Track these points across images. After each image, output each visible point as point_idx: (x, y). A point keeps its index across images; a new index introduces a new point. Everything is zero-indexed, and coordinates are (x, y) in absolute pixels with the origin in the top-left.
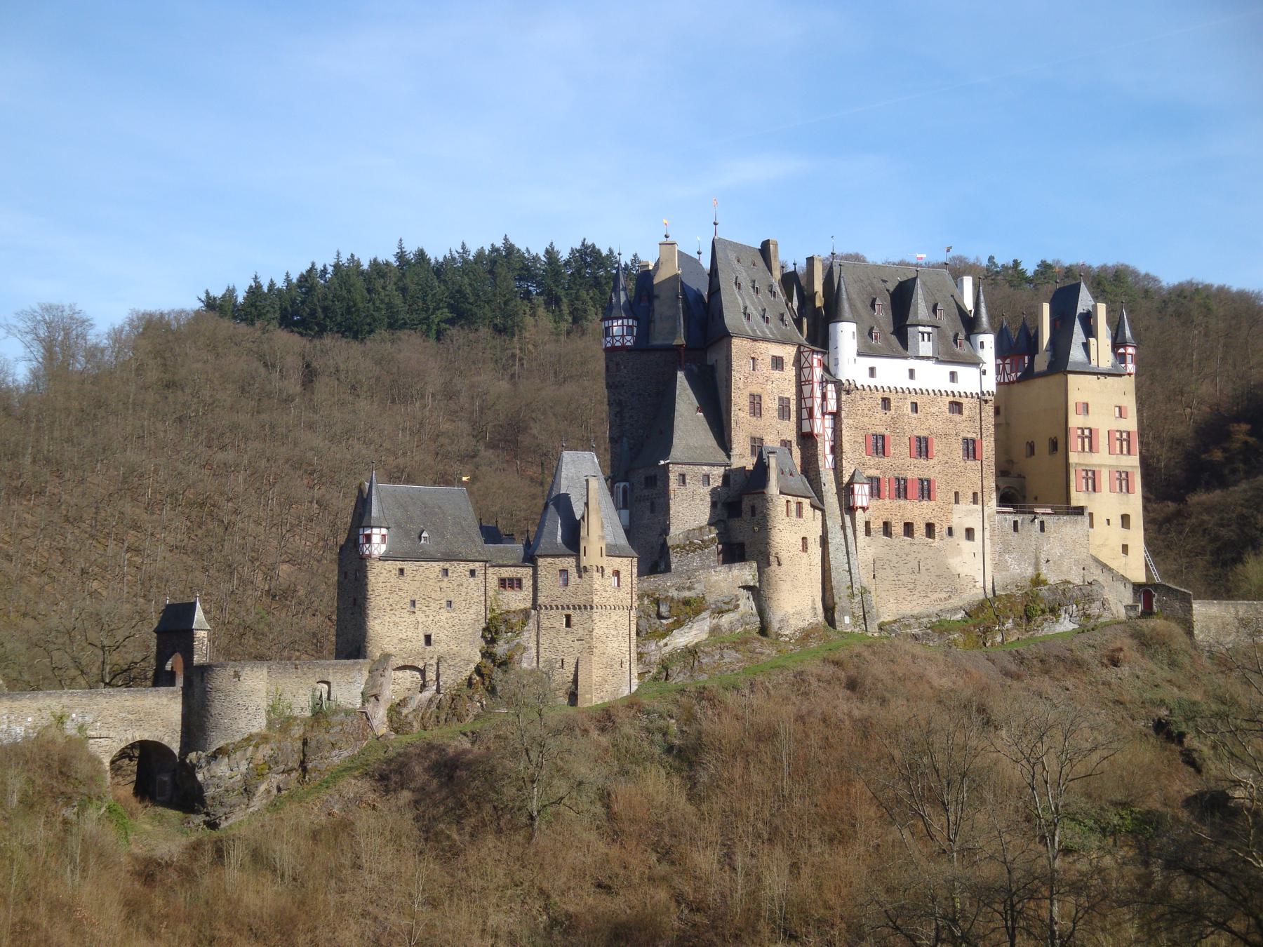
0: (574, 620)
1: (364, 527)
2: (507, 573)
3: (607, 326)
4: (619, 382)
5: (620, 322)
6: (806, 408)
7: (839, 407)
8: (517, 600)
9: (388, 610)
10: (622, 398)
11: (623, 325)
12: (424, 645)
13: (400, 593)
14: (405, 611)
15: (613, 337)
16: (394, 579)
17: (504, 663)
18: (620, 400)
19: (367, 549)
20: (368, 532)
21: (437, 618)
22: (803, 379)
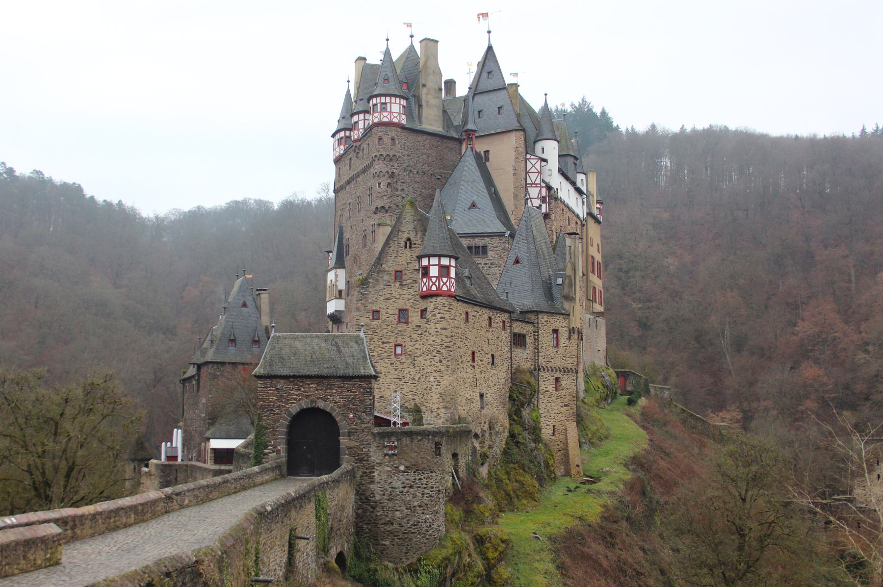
0: (563, 383)
1: (440, 256)
2: (518, 328)
4: (394, 155)
5: (398, 100)
8: (523, 357)
9: (460, 363)
10: (395, 171)
11: (400, 104)
12: (480, 407)
14: (469, 364)
15: (391, 112)
16: (463, 326)
18: (393, 173)
19: (445, 284)
20: (445, 261)
21: (487, 373)
22: (529, 181)
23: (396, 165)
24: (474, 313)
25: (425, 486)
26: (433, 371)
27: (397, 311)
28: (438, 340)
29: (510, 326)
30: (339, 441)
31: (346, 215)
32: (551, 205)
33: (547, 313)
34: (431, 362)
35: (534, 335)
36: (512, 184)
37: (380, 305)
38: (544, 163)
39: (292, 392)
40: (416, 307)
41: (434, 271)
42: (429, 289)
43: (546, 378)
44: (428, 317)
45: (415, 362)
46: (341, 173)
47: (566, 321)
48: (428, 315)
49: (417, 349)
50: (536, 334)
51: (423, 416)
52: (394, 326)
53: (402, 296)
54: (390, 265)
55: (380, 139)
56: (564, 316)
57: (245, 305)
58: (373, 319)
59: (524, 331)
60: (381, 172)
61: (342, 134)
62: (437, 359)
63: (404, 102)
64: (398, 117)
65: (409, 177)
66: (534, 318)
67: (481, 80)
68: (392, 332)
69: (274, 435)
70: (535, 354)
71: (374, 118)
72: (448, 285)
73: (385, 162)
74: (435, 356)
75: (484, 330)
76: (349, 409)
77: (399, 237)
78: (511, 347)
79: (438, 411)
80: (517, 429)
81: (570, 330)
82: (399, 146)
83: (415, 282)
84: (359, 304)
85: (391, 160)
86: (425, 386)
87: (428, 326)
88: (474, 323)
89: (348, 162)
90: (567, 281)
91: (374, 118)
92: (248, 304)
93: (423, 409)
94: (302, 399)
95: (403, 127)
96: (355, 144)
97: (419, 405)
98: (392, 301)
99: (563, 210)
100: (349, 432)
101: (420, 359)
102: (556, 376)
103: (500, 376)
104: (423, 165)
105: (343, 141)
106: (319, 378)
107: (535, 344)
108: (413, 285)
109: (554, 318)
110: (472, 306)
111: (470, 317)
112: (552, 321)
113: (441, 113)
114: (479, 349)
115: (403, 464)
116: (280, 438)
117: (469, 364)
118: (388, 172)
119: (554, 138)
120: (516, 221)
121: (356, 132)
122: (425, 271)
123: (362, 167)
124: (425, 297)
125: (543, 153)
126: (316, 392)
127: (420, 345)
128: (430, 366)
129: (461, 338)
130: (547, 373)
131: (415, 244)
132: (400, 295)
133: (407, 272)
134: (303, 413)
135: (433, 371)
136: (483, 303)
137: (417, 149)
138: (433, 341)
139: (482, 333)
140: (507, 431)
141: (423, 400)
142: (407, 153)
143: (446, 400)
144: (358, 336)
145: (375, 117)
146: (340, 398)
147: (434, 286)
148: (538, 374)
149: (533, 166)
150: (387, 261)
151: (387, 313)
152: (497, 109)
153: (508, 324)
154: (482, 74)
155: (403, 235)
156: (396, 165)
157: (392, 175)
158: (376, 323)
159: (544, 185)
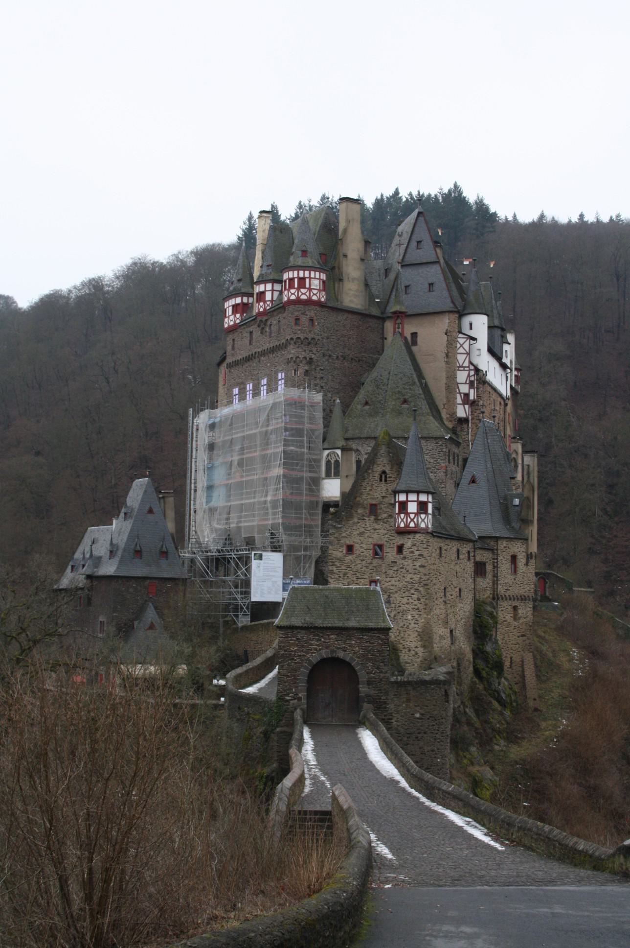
0: (520, 612)
1: (418, 492)
3: (301, 275)
4: (313, 339)
5: (317, 274)
6: (460, 393)
7: (477, 397)
10: (313, 356)
11: (320, 279)
13: (440, 577)
15: (310, 289)
16: (437, 561)
17: (498, 666)
18: (311, 359)
19: (423, 520)
20: (423, 498)
23: (314, 350)
24: (445, 548)
25: (437, 732)
26: (411, 610)
27: (371, 546)
28: (416, 578)
29: (474, 556)
30: (359, 689)
32: (480, 391)
33: (506, 538)
34: (408, 600)
35: (494, 562)
36: (444, 374)
37: (354, 540)
38: (472, 342)
39: (313, 642)
40: (392, 542)
41: (412, 508)
42: (407, 526)
43: (504, 607)
44: (404, 553)
45: (391, 599)
46: (236, 345)
47: (524, 546)
48: (406, 551)
49: (393, 585)
50: (495, 561)
51: (400, 654)
52: (369, 561)
53: (378, 531)
55: (297, 320)
56: (522, 541)
57: (150, 511)
58: (347, 554)
59: (484, 558)
60: (298, 357)
61: (238, 300)
62: (415, 597)
63: (324, 277)
64: (318, 295)
65: (328, 363)
66: (493, 544)
67: (409, 250)
68: (367, 567)
69: (295, 683)
70: (493, 582)
71: (290, 294)
72: (426, 522)
73: (302, 345)
74: (413, 594)
75: (453, 563)
76: (368, 659)
77: (375, 470)
78: (474, 578)
79: (416, 650)
80: (481, 665)
81: (528, 555)
82: (318, 327)
83: (391, 516)
84: (332, 538)
85: (309, 344)
86: (402, 624)
87: (406, 563)
88: (446, 558)
89: (248, 335)
91: (290, 294)
92: (155, 510)
93: (401, 646)
94: (323, 650)
96: (259, 319)
97: (395, 642)
98: (366, 535)
99: (489, 392)
100: (368, 681)
101: (396, 595)
102: (514, 605)
103: (465, 609)
104: (343, 348)
105: (240, 308)
106: (340, 630)
107: (494, 571)
108: (389, 520)
109: (512, 543)
110: (444, 540)
111: (443, 552)
112: (510, 546)
113: (362, 288)
114: (450, 583)
115: (419, 712)
116: (301, 686)
117: (441, 600)
118: (305, 358)
119: (484, 312)
120: (448, 416)
121: (261, 304)
123: (267, 346)
124: (402, 532)
125: (471, 328)
126: (336, 643)
127: (395, 581)
128: (408, 603)
129: (436, 574)
130: (505, 602)
131: (390, 477)
132: (375, 530)
133: (383, 506)
134: (323, 661)
135: (411, 610)
136: (453, 536)
137: (337, 331)
138: (411, 579)
139: (452, 567)
140: (471, 666)
141: (399, 638)
142: (326, 335)
143: (425, 639)
144: (375, 591)
145: (292, 294)
146: (359, 648)
147: (412, 523)
148: (497, 603)
149: (461, 346)
150: (361, 494)
151: (361, 547)
152: (428, 286)
153: (472, 554)
154: (411, 243)
155: (379, 468)
156: (314, 350)
157: (310, 362)
158: (350, 557)
159: (472, 367)
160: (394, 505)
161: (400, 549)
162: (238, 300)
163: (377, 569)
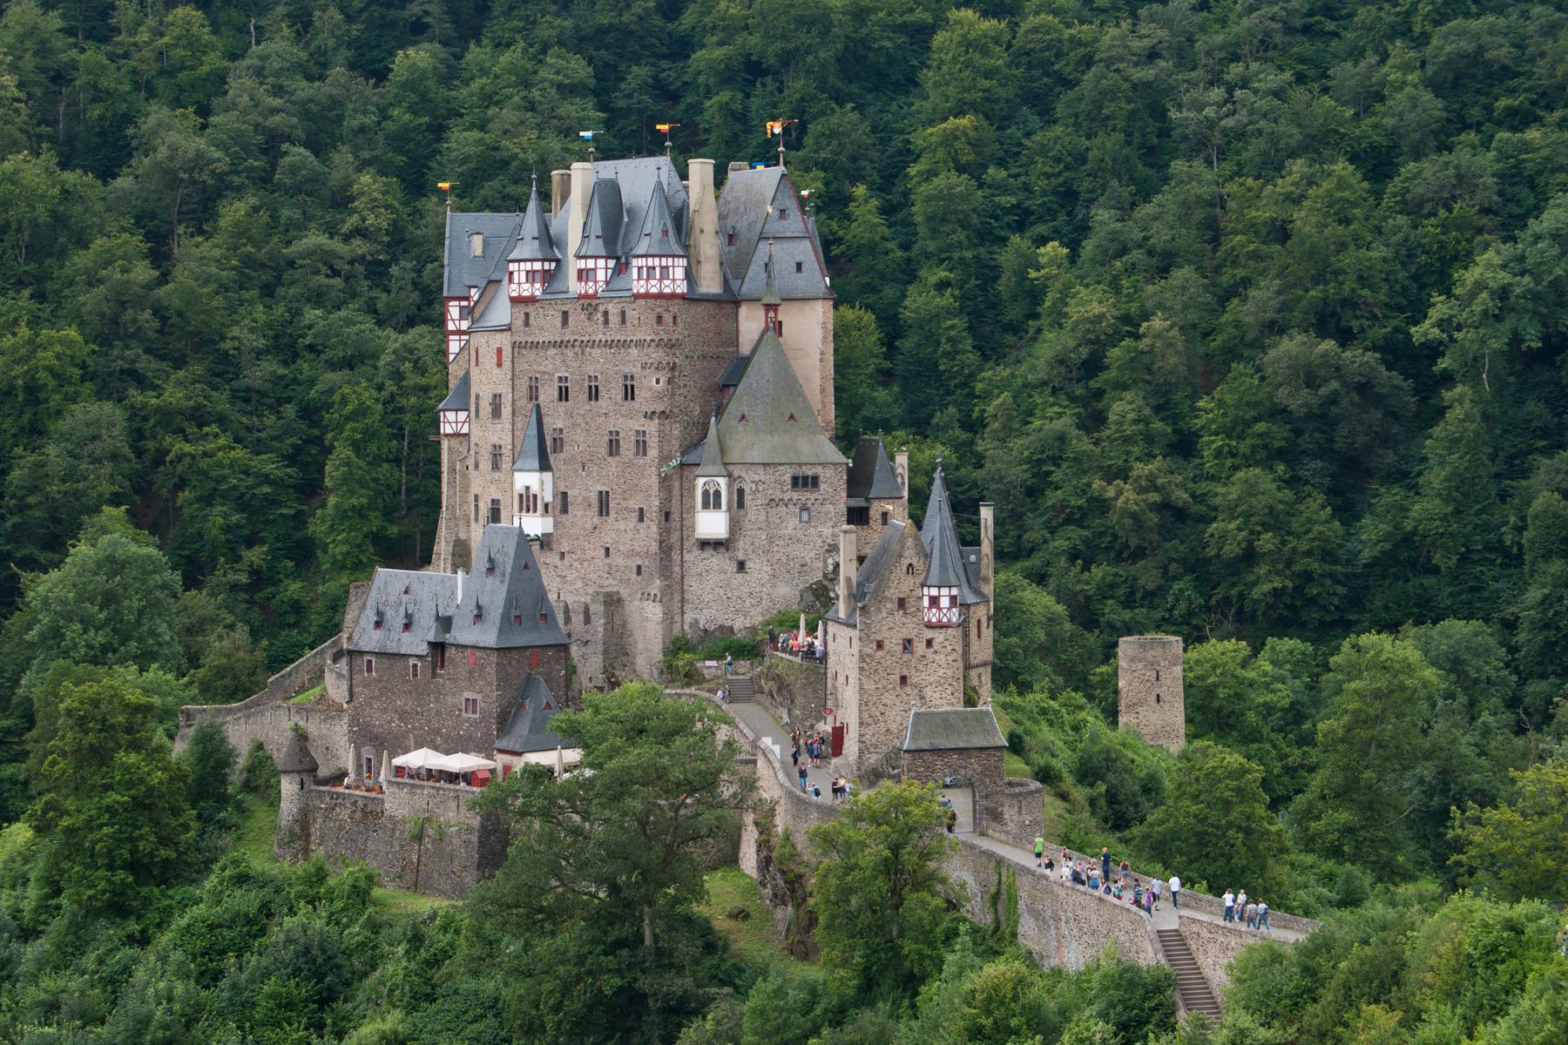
20: (954, 591)
31: (548, 394)
36: (818, 375)
37: (884, 634)
41: (945, 602)
42: (940, 621)
48: (936, 645)
54: (893, 593)
55: (659, 319)
57: (526, 567)
61: (537, 266)
90: (985, 561)
95: (682, 297)
105: (538, 276)
106: (960, 750)
122: (934, 601)
124: (930, 626)
144: (987, 713)
157: (673, 369)
158: (880, 653)
160: (921, 598)
161: (929, 643)
162: (537, 266)
163: (907, 664)
